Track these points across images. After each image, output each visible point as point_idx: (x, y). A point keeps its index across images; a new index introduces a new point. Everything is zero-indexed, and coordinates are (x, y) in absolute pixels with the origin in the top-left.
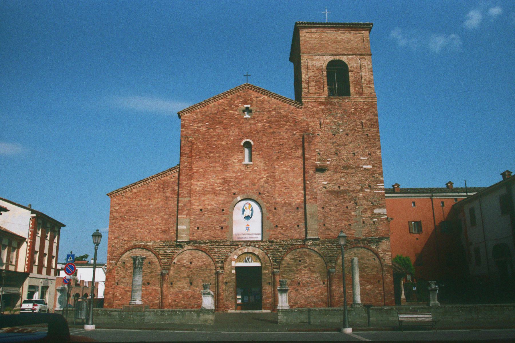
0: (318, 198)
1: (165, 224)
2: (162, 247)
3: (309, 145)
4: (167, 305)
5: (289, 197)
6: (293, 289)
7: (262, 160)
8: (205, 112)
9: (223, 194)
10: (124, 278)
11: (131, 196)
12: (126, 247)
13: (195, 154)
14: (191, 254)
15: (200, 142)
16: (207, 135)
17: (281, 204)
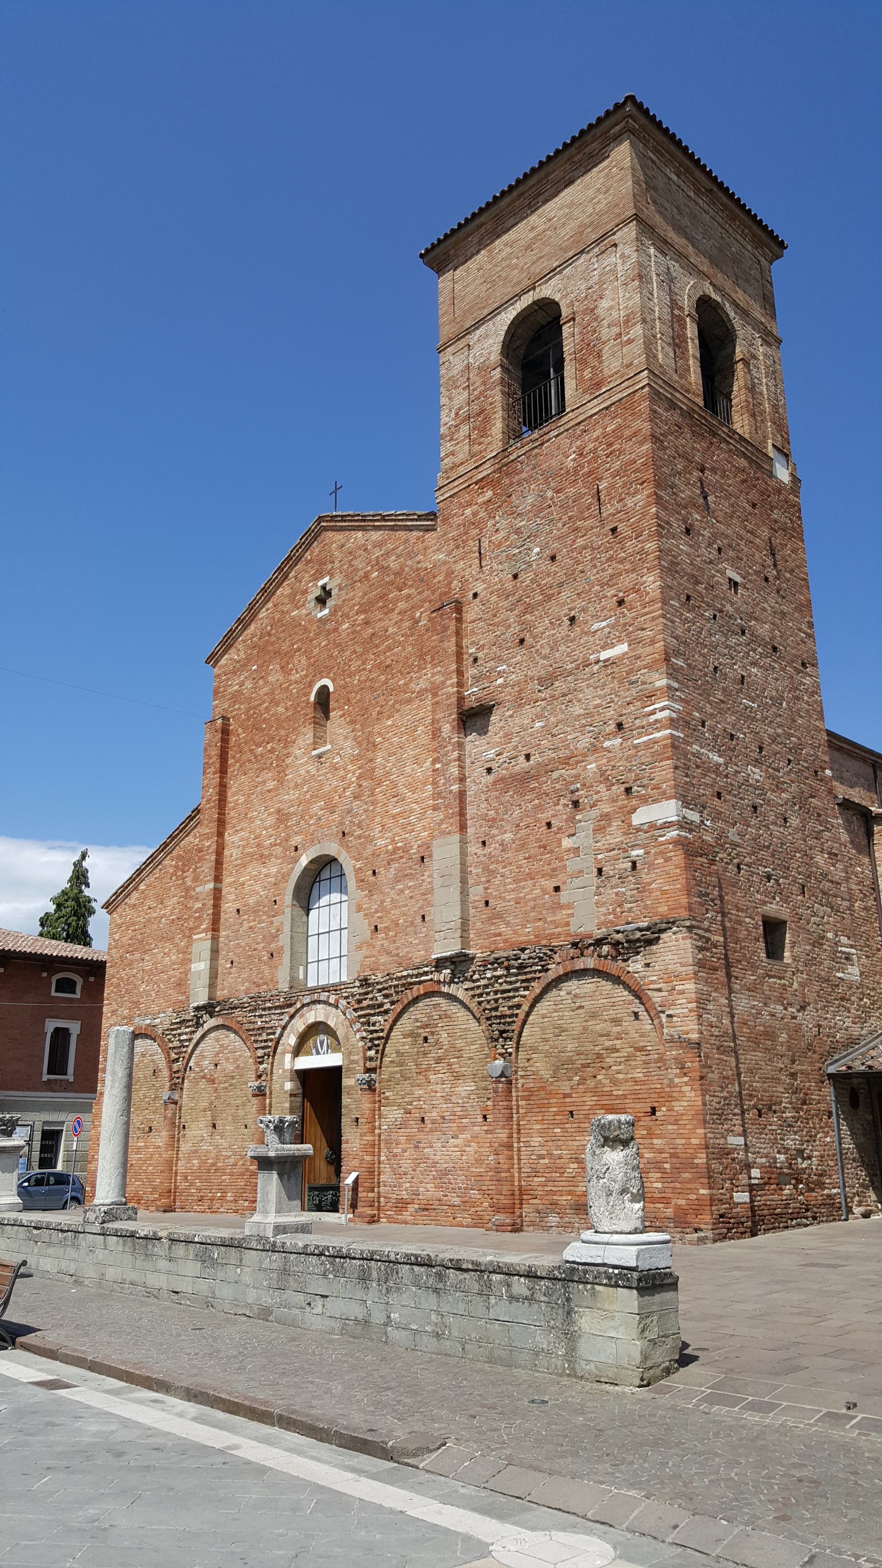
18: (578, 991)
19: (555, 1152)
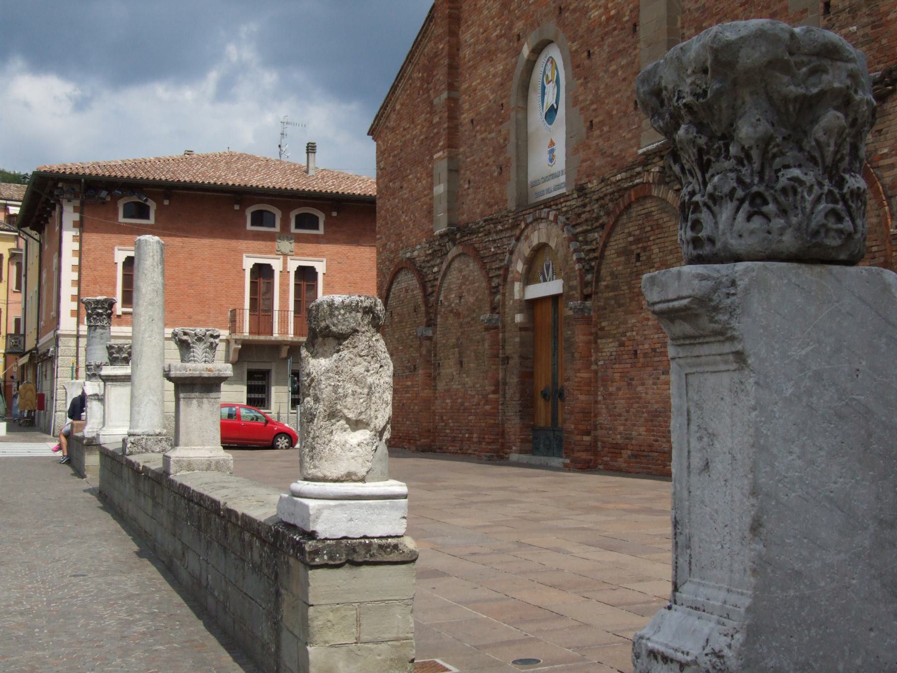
4: (429, 431)
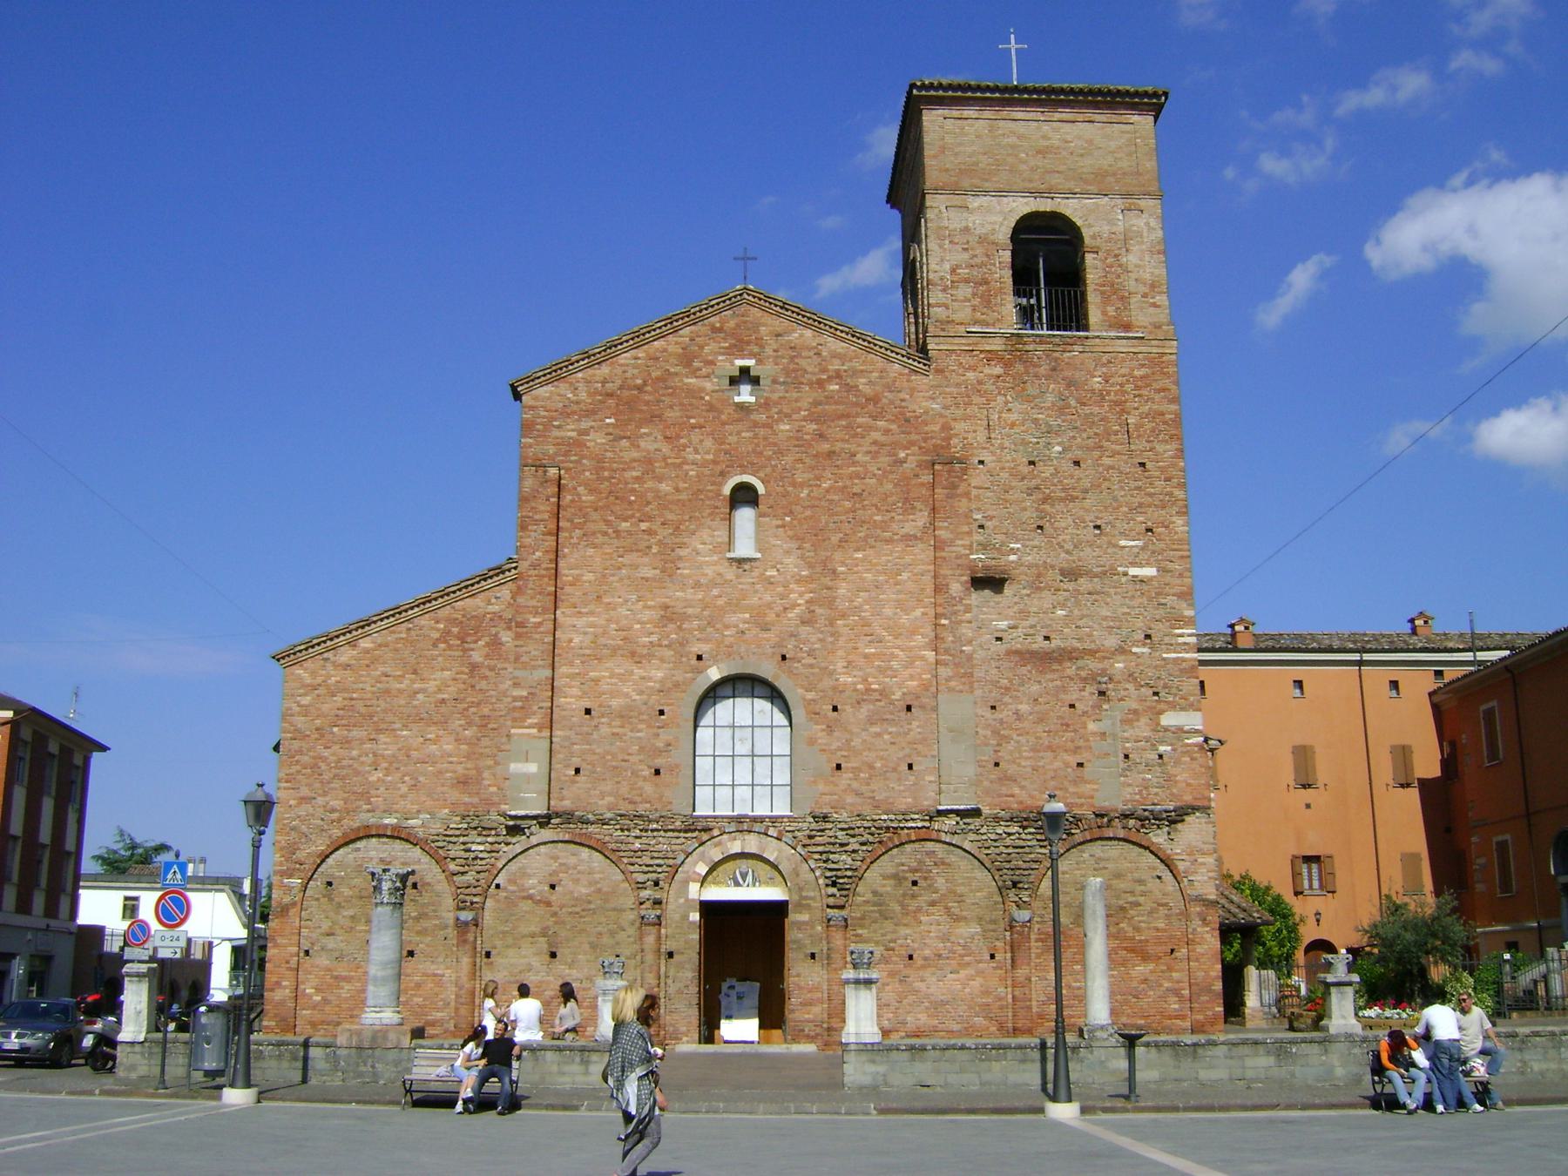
0: (979, 673)
1: (468, 757)
2: (458, 832)
3: (949, 497)
5: (881, 670)
6: (892, 974)
7: (794, 545)
8: (604, 382)
9: (662, 660)
10: (328, 935)
11: (354, 662)
12: (337, 833)
13: (568, 524)
14: (555, 858)
15: (586, 485)
16: (612, 460)
17: (855, 693)
18: (1102, 854)
19: (1074, 984)
